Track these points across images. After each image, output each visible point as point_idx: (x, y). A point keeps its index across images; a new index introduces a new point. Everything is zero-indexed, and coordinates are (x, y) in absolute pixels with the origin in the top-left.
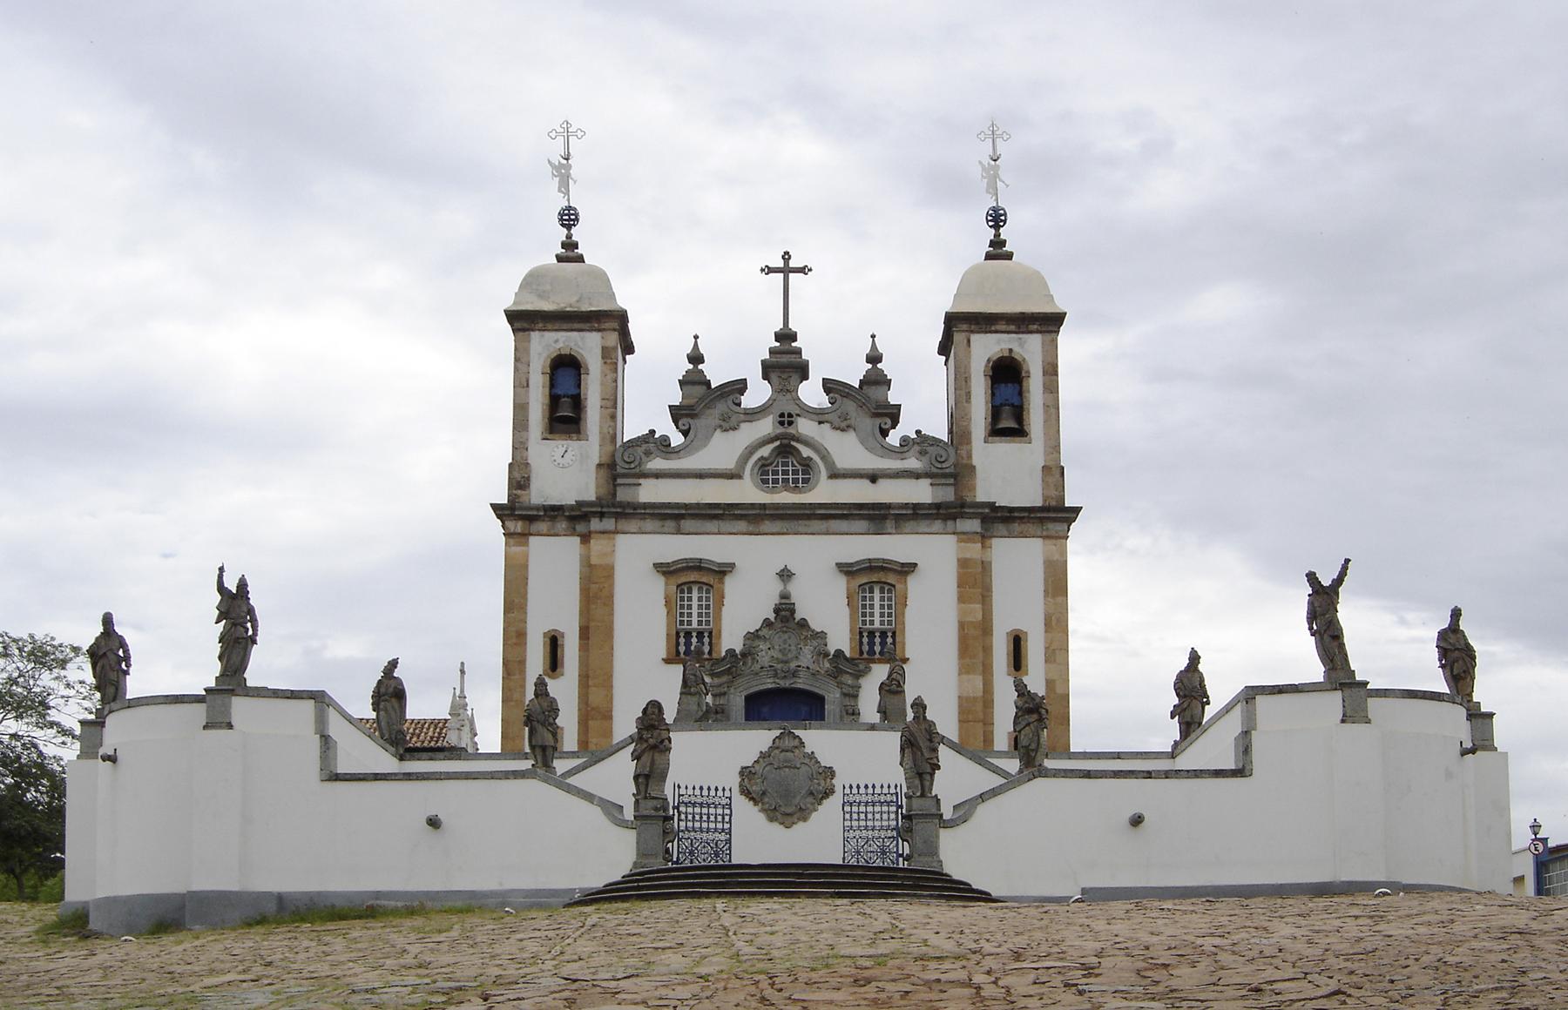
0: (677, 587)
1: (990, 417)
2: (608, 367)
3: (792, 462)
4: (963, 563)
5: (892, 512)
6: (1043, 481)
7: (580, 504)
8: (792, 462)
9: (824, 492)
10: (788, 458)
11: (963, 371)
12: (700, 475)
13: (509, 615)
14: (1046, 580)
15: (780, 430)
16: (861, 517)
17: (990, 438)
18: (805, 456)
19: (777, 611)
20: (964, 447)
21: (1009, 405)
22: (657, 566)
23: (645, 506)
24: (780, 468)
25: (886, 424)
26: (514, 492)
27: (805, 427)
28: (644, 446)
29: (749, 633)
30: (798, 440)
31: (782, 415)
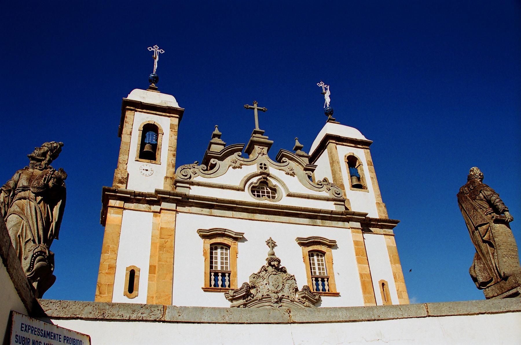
0: (211, 245)
2: (173, 133)
4: (356, 243)
7: (158, 192)
9: (285, 201)
12: (222, 187)
13: (106, 254)
14: (390, 256)
15: (261, 170)
18: (274, 184)
22: (200, 231)
23: (194, 198)
27: (273, 170)
28: (192, 169)
30: (270, 177)
31: (261, 164)
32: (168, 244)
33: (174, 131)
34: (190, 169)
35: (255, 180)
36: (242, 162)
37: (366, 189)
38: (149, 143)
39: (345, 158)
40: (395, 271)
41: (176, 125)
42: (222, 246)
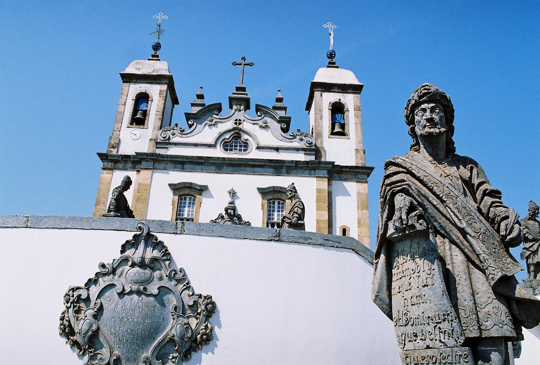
1: (331, 127)
3: (239, 141)
4: (319, 191)
5: (286, 164)
6: (355, 156)
8: (239, 141)
9: (253, 154)
10: (238, 140)
11: (319, 107)
12: (196, 145)
14: (358, 202)
15: (236, 126)
16: (270, 167)
17: (331, 136)
19: (226, 210)
20: (319, 139)
21: (339, 123)
22: (170, 185)
24: (234, 144)
25: (284, 126)
26: (110, 149)
27: (246, 126)
28: (172, 131)
29: (211, 221)
31: (236, 120)
32: (143, 197)
33: (163, 97)
34: (170, 131)
35: (227, 136)
36: (218, 120)
37: (347, 136)
38: (141, 110)
39: (329, 106)
40: (360, 217)
41: (164, 91)
42: (191, 197)
